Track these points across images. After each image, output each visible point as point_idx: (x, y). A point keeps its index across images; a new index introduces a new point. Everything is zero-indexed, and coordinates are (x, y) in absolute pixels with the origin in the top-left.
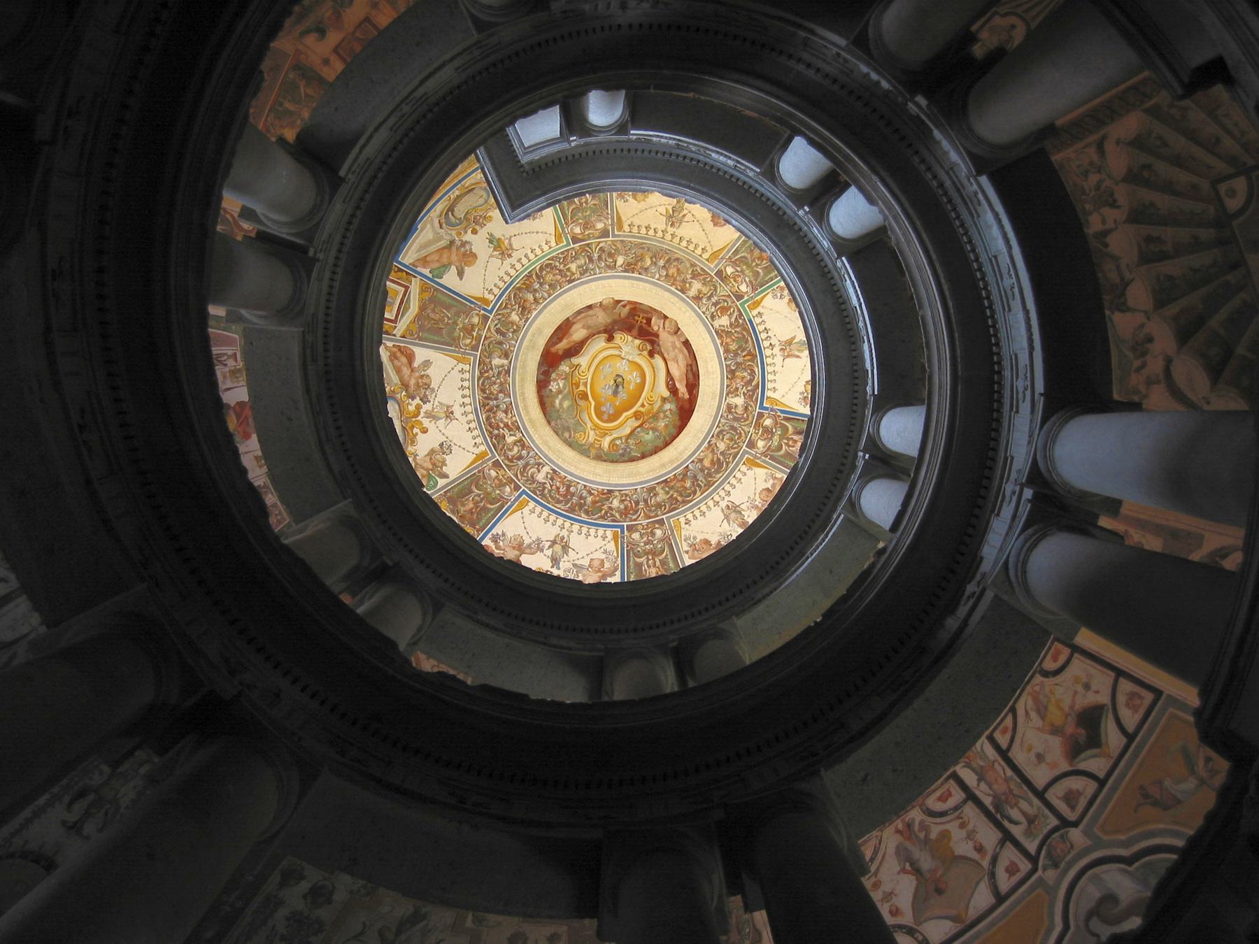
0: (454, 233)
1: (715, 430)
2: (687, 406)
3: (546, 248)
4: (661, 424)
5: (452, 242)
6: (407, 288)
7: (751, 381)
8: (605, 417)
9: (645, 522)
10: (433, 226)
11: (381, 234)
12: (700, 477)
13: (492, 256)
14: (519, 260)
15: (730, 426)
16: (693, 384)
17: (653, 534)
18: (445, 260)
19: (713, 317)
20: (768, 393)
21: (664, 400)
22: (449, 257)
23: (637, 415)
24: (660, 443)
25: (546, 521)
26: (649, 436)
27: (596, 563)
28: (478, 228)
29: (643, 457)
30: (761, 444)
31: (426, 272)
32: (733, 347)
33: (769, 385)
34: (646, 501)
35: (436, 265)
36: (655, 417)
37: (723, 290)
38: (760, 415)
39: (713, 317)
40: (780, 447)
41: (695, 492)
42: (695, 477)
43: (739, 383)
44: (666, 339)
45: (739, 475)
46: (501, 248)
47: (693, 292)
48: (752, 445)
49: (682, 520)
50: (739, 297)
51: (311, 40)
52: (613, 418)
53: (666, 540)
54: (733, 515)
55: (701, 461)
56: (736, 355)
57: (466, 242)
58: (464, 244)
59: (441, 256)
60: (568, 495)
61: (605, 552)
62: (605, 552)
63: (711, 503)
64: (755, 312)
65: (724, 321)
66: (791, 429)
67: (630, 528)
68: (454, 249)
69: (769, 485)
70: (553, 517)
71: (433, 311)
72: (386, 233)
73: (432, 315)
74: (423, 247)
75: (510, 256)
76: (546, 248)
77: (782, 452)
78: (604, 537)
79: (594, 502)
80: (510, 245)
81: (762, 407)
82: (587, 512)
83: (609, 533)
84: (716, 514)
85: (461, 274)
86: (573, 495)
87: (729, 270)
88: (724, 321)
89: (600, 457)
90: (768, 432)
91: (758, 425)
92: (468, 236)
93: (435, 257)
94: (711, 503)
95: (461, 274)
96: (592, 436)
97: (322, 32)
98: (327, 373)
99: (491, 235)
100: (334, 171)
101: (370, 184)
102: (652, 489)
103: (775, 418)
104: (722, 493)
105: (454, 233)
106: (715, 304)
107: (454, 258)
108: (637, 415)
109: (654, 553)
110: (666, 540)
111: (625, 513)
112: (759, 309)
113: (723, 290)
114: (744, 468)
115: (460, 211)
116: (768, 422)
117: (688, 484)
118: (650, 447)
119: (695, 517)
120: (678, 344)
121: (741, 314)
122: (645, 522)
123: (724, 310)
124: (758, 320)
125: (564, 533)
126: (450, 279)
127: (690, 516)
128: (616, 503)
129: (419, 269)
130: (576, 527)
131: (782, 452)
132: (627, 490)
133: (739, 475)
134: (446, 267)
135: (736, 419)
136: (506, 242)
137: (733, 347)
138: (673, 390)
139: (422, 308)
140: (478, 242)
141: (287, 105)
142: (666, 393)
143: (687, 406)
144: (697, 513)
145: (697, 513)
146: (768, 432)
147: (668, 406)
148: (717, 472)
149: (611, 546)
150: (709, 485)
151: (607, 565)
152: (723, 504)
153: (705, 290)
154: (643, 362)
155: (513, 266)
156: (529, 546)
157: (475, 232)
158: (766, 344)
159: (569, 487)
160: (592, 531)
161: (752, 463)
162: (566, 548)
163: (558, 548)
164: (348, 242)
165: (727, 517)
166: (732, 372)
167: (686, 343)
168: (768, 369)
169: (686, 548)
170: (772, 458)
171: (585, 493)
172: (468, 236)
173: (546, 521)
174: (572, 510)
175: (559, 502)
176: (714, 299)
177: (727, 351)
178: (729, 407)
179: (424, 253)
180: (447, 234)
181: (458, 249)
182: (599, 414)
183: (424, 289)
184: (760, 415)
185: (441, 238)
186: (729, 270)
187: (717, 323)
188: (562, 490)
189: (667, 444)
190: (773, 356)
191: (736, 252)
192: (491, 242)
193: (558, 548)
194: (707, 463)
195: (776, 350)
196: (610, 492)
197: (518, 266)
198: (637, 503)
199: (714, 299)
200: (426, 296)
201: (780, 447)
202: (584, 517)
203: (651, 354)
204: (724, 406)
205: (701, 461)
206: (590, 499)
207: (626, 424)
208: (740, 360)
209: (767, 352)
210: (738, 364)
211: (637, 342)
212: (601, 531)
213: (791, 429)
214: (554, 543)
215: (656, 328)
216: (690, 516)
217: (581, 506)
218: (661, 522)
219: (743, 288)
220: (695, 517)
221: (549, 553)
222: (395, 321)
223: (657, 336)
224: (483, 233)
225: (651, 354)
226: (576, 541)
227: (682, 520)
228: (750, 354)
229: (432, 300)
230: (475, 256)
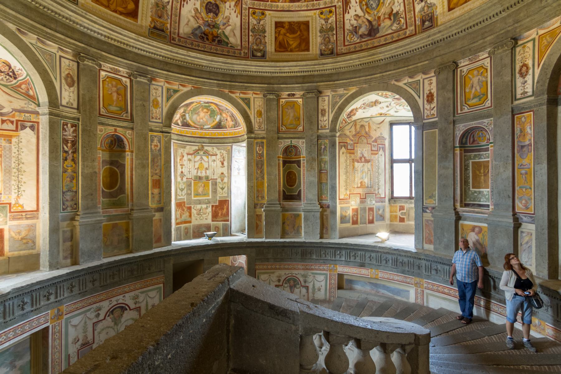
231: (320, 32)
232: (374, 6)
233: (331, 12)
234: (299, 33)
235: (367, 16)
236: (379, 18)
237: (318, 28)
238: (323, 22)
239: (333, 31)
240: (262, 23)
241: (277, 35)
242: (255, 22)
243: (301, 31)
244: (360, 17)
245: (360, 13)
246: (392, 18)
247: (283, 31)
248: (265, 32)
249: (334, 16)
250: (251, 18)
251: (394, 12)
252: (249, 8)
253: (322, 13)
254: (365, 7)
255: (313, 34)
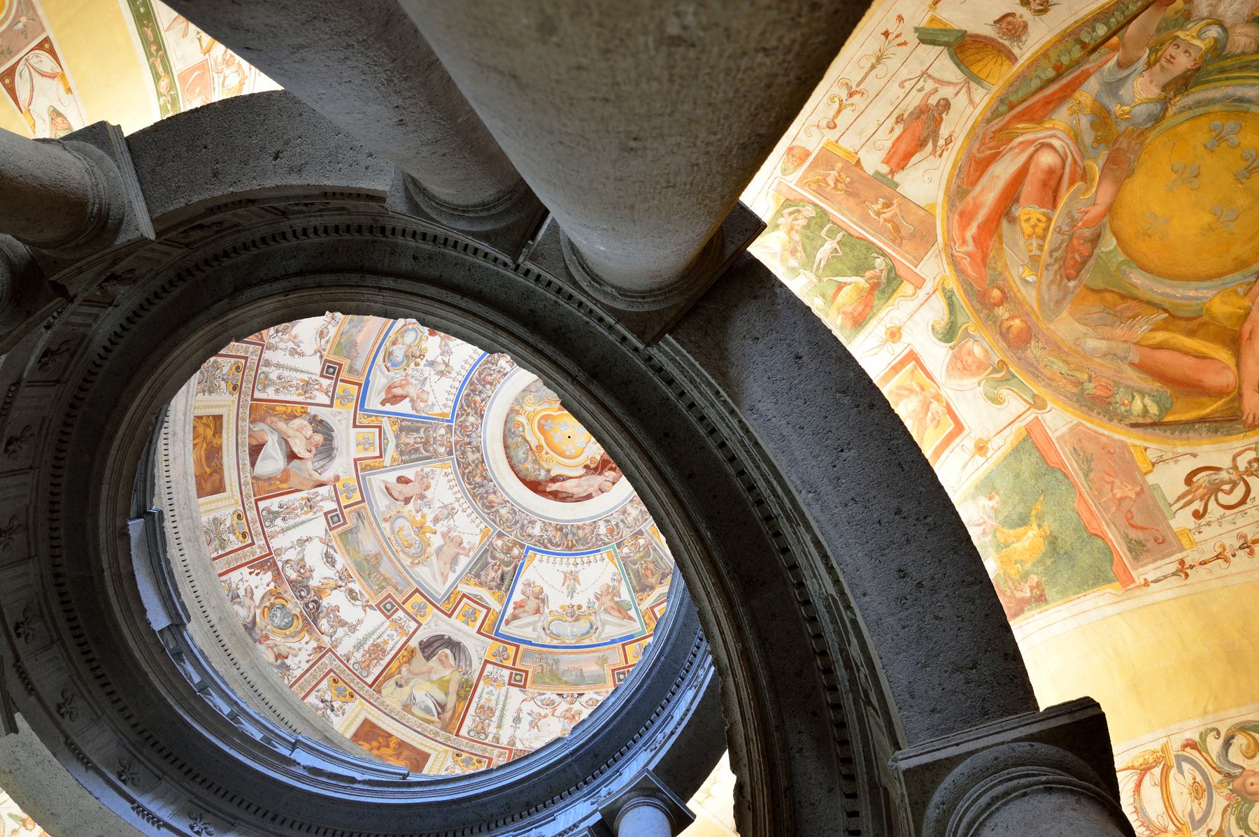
1: (517, 508)
2: (540, 488)
4: (529, 465)
7: (551, 543)
8: (543, 422)
9: (453, 440)
11: (574, 369)
12: (482, 490)
15: (519, 519)
16: (555, 495)
17: (442, 445)
19: (608, 521)
20: (539, 555)
21: (549, 471)
23: (540, 447)
24: (515, 461)
25: (466, 362)
26: (521, 454)
27: (425, 396)
29: (506, 447)
30: (499, 543)
32: (581, 533)
33: (545, 557)
34: (470, 443)
36: (536, 462)
37: (627, 533)
38: (522, 546)
39: (608, 521)
40: (493, 558)
41: (470, 484)
42: (483, 486)
43: (551, 532)
44: (597, 480)
45: (478, 521)
47: (630, 509)
48: (500, 535)
49: (449, 470)
50: (619, 545)
51: (937, 311)
52: (541, 428)
53: (435, 455)
54: (446, 512)
55: (495, 493)
56: (574, 535)
60: (485, 383)
61: (433, 405)
62: (433, 405)
63: (459, 495)
64: (605, 556)
65: (602, 530)
66: (506, 569)
67: (450, 427)
69: (465, 544)
70: (468, 368)
72: (574, 379)
77: (490, 560)
78: (445, 405)
79: (475, 402)
81: (529, 548)
82: (468, 395)
83: (449, 410)
84: (449, 498)
86: (484, 386)
87: (642, 542)
88: (602, 530)
89: (512, 412)
90: (508, 551)
91: (515, 543)
94: (459, 495)
96: (529, 409)
97: (949, 334)
98: (383, 230)
100: (673, 328)
101: (660, 370)
102: (478, 449)
103: (519, 558)
104: (465, 506)
106: (617, 525)
108: (540, 447)
109: (426, 443)
110: (435, 455)
111: (462, 426)
112: (607, 560)
113: (627, 533)
114: (482, 526)
116: (516, 551)
117: (478, 479)
118: (513, 453)
119: (449, 481)
120: (591, 490)
121: (605, 544)
122: (453, 440)
123: (611, 531)
124: (598, 556)
125: (454, 374)
127: (451, 477)
128: (471, 419)
130: (458, 385)
131: (490, 560)
132: (481, 431)
133: (478, 521)
135: (522, 527)
137: (581, 533)
138: (554, 480)
141: (829, 245)
142: (553, 474)
143: (540, 488)
144: (453, 483)
145: (453, 483)
146: (508, 551)
147: (543, 473)
148: (483, 504)
149: (437, 410)
150: (474, 496)
151: (422, 405)
152: (456, 505)
153: (630, 519)
154: (583, 459)
156: (447, 345)
158: (579, 560)
159: (491, 384)
160: (453, 397)
161: (485, 534)
162: (441, 374)
163: (442, 367)
164: (571, 308)
165: (445, 507)
166: (561, 530)
167: (589, 497)
168: (558, 558)
169: (427, 470)
170: (486, 551)
171: (483, 396)
173: (466, 362)
174: (472, 383)
175: (480, 374)
176: (621, 525)
177: (578, 528)
178: (532, 522)
182: (546, 417)
184: (522, 546)
186: (642, 542)
187: (602, 524)
188: (489, 379)
189: (512, 467)
190: (568, 565)
191: (655, 549)
193: (442, 367)
194: (492, 497)
195: (572, 568)
196: (482, 416)
198: (469, 436)
199: (621, 525)
201: (493, 558)
202: (464, 392)
203: (586, 467)
204: (534, 518)
205: (495, 493)
206: (478, 399)
207: (534, 437)
208: (570, 537)
209: (572, 560)
210: (567, 535)
211: (598, 458)
212: (451, 404)
213: (506, 569)
214: (447, 365)
215: (607, 474)
216: (451, 477)
217: (473, 391)
218: (450, 453)
219: (626, 550)
220: (449, 481)
221: (439, 360)
223: (600, 474)
225: (586, 467)
226: (446, 383)
227: (449, 470)
228: (573, 546)
231: (215, 519)
232: (277, 621)
233: (244, 536)
234: (208, 470)
235: (258, 612)
236: (267, 638)
237: (218, 515)
238: (228, 524)
239: (223, 549)
240: (223, 383)
241: (204, 420)
242: (225, 370)
243: (211, 475)
244: (252, 598)
245: (258, 595)
246: (279, 661)
247: (210, 432)
248: (211, 392)
249: (240, 545)
250: (233, 360)
251: (288, 662)
252: (246, 358)
253: (239, 516)
254: (268, 604)
255: (210, 503)
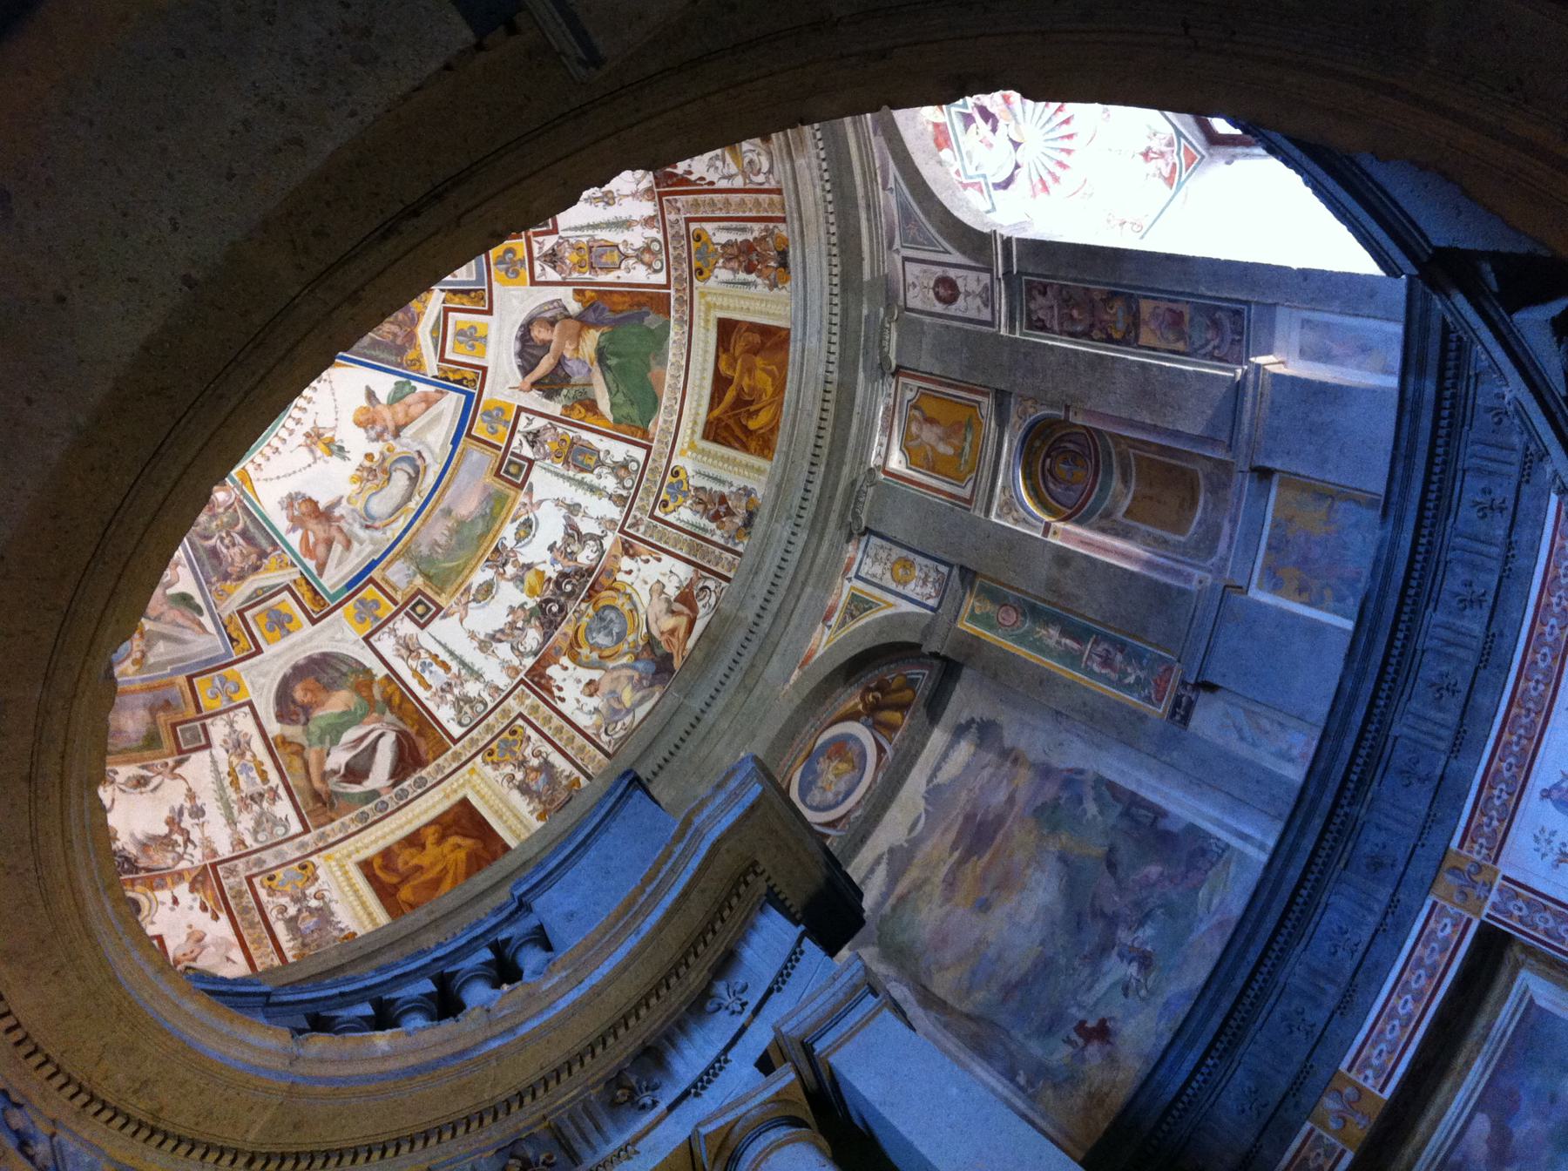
0: (399, 449)
3: (259, 459)
5: (397, 435)
6: (442, 359)
10: (432, 452)
13: (334, 429)
14: (291, 432)
18: (399, 408)
22: (394, 414)
28: (367, 464)
31: (421, 388)
35: (409, 399)
46: (323, 443)
57: (373, 440)
58: (379, 437)
59: (407, 414)
68: (391, 426)
71: (395, 335)
73: (395, 329)
74: (437, 418)
75: (308, 435)
76: (259, 459)
80: (312, 451)
85: (370, 395)
92: (376, 448)
93: (414, 411)
95: (370, 395)
99: (344, 458)
105: (399, 449)
107: (387, 414)
115: (400, 480)
126: (384, 384)
129: (431, 389)
134: (395, 398)
136: (319, 453)
139: (411, 337)
140: (358, 443)
155: (298, 422)
157: (369, 456)
172: (376, 448)
179: (433, 410)
180: (407, 443)
181: (385, 429)
183: (417, 362)
185: (415, 437)
192: (341, 449)
197: (290, 424)
200: (411, 355)
222: (447, 311)
224: (356, 458)
229: (401, 350)
230: (359, 424)
